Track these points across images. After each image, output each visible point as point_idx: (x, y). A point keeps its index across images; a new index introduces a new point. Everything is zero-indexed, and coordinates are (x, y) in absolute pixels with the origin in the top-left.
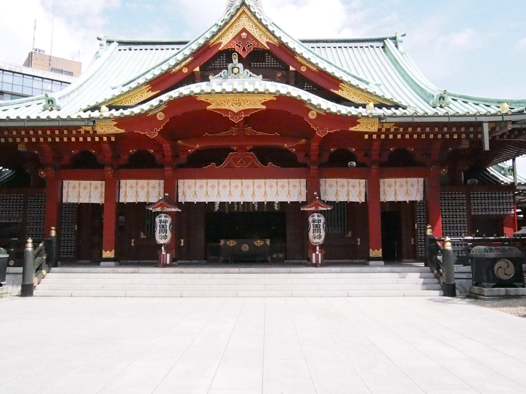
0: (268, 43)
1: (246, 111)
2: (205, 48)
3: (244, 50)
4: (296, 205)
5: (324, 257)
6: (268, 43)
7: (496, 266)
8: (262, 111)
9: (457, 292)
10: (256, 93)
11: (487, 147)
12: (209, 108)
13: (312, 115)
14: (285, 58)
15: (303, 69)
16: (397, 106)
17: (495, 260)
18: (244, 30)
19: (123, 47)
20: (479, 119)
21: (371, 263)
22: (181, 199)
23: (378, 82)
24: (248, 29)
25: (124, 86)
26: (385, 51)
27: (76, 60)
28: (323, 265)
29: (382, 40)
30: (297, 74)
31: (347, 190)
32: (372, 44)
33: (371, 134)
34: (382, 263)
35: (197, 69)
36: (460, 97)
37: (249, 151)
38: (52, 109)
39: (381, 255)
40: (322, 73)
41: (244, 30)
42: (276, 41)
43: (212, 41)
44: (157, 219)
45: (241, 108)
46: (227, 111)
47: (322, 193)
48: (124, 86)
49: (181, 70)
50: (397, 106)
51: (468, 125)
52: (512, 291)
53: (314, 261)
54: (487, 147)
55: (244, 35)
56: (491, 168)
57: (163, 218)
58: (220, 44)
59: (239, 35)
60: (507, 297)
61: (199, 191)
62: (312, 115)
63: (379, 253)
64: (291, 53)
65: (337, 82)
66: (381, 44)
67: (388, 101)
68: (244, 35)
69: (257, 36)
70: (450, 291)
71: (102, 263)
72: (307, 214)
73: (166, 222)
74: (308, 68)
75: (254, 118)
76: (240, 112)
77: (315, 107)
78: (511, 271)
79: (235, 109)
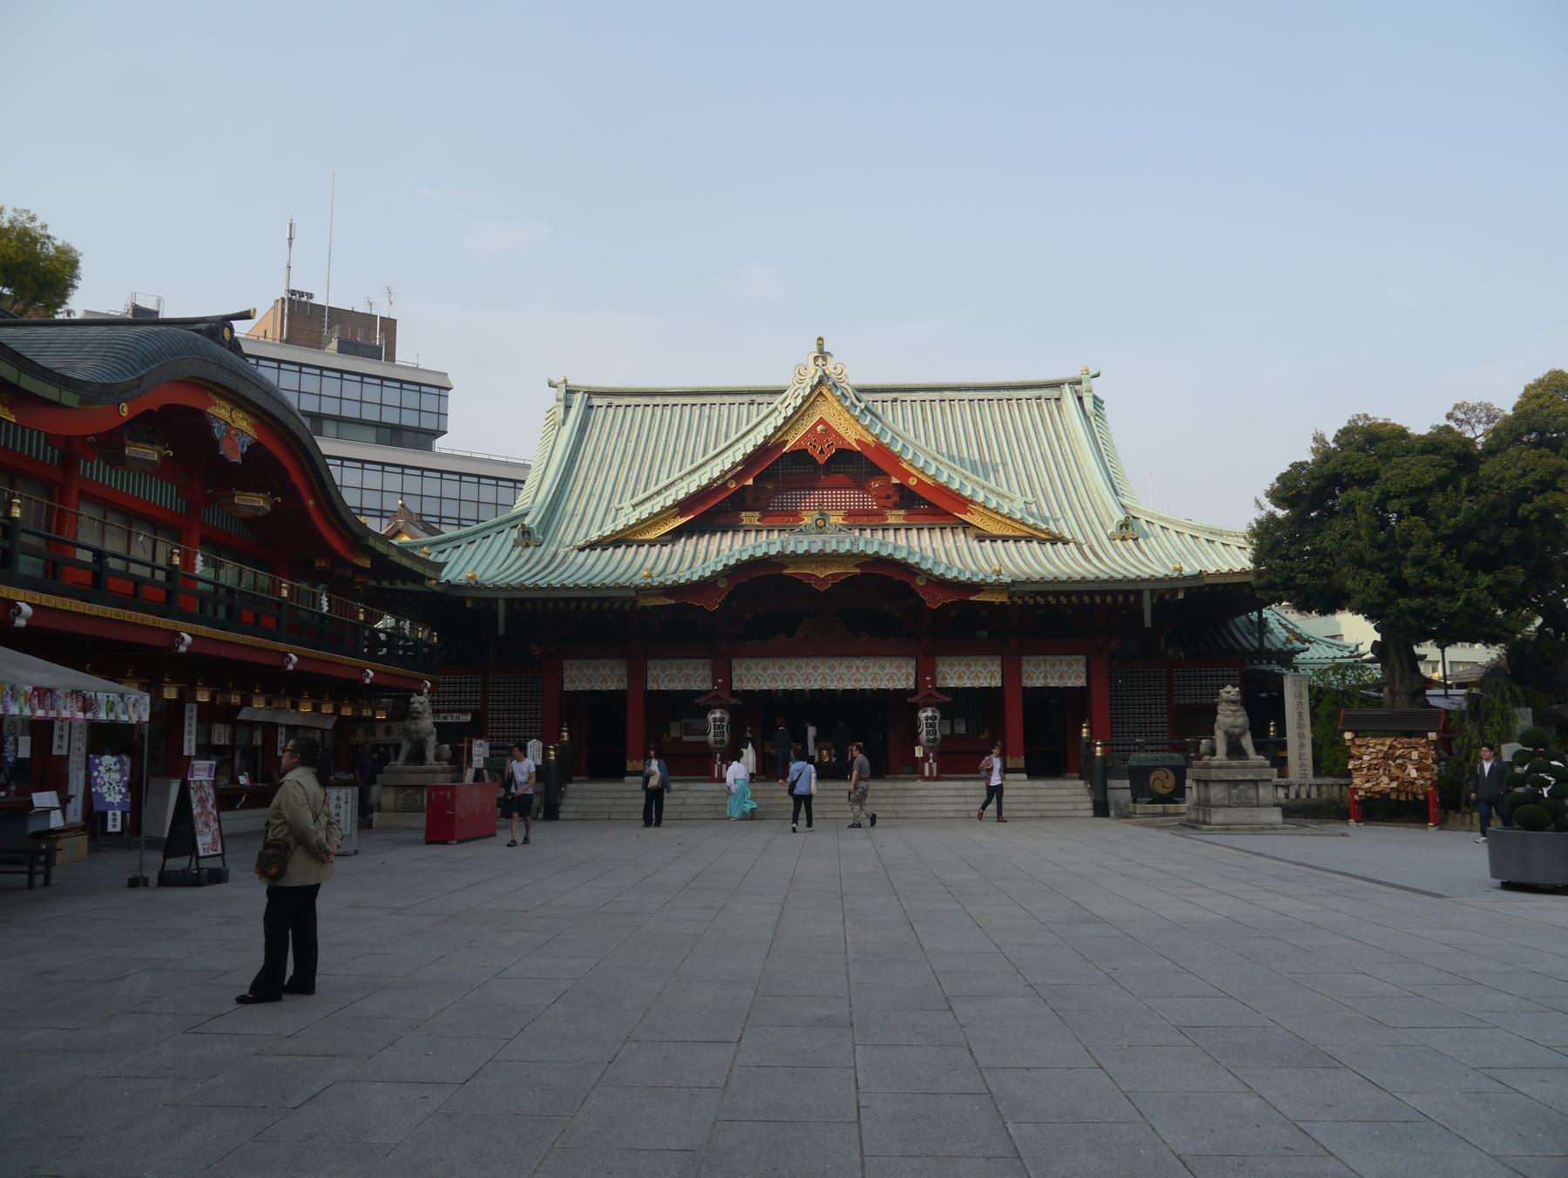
0: (858, 441)
2: (762, 451)
3: (822, 452)
5: (941, 770)
6: (858, 441)
7: (1152, 778)
8: (856, 575)
9: (1112, 813)
10: (849, 555)
11: (1148, 623)
13: (920, 582)
14: (884, 465)
15: (912, 482)
16: (1055, 540)
17: (1152, 769)
18: (821, 421)
19: (596, 401)
20: (1140, 587)
22: (736, 686)
23: (1030, 498)
24: (828, 419)
25: (634, 506)
26: (1059, 409)
27: (381, 311)
28: (938, 779)
29: (1057, 385)
30: (902, 488)
32: (1037, 393)
33: (1002, 603)
34: (1025, 776)
35: (750, 482)
36: (1160, 519)
38: (527, 546)
39: (1022, 765)
40: (943, 490)
41: (821, 421)
42: (870, 438)
44: (711, 717)
47: (939, 677)
48: (634, 506)
49: (725, 484)
50: (1055, 540)
51: (1126, 593)
52: (1171, 807)
53: (927, 773)
54: (1148, 623)
55: (820, 428)
56: (1237, 620)
57: (718, 715)
60: (1165, 814)
63: (1021, 762)
64: (895, 459)
65: (964, 503)
66: (1054, 393)
67: (1042, 531)
69: (841, 431)
70: (1101, 809)
71: (627, 779)
72: (916, 708)
73: (722, 720)
77: (924, 572)
78: (1171, 782)
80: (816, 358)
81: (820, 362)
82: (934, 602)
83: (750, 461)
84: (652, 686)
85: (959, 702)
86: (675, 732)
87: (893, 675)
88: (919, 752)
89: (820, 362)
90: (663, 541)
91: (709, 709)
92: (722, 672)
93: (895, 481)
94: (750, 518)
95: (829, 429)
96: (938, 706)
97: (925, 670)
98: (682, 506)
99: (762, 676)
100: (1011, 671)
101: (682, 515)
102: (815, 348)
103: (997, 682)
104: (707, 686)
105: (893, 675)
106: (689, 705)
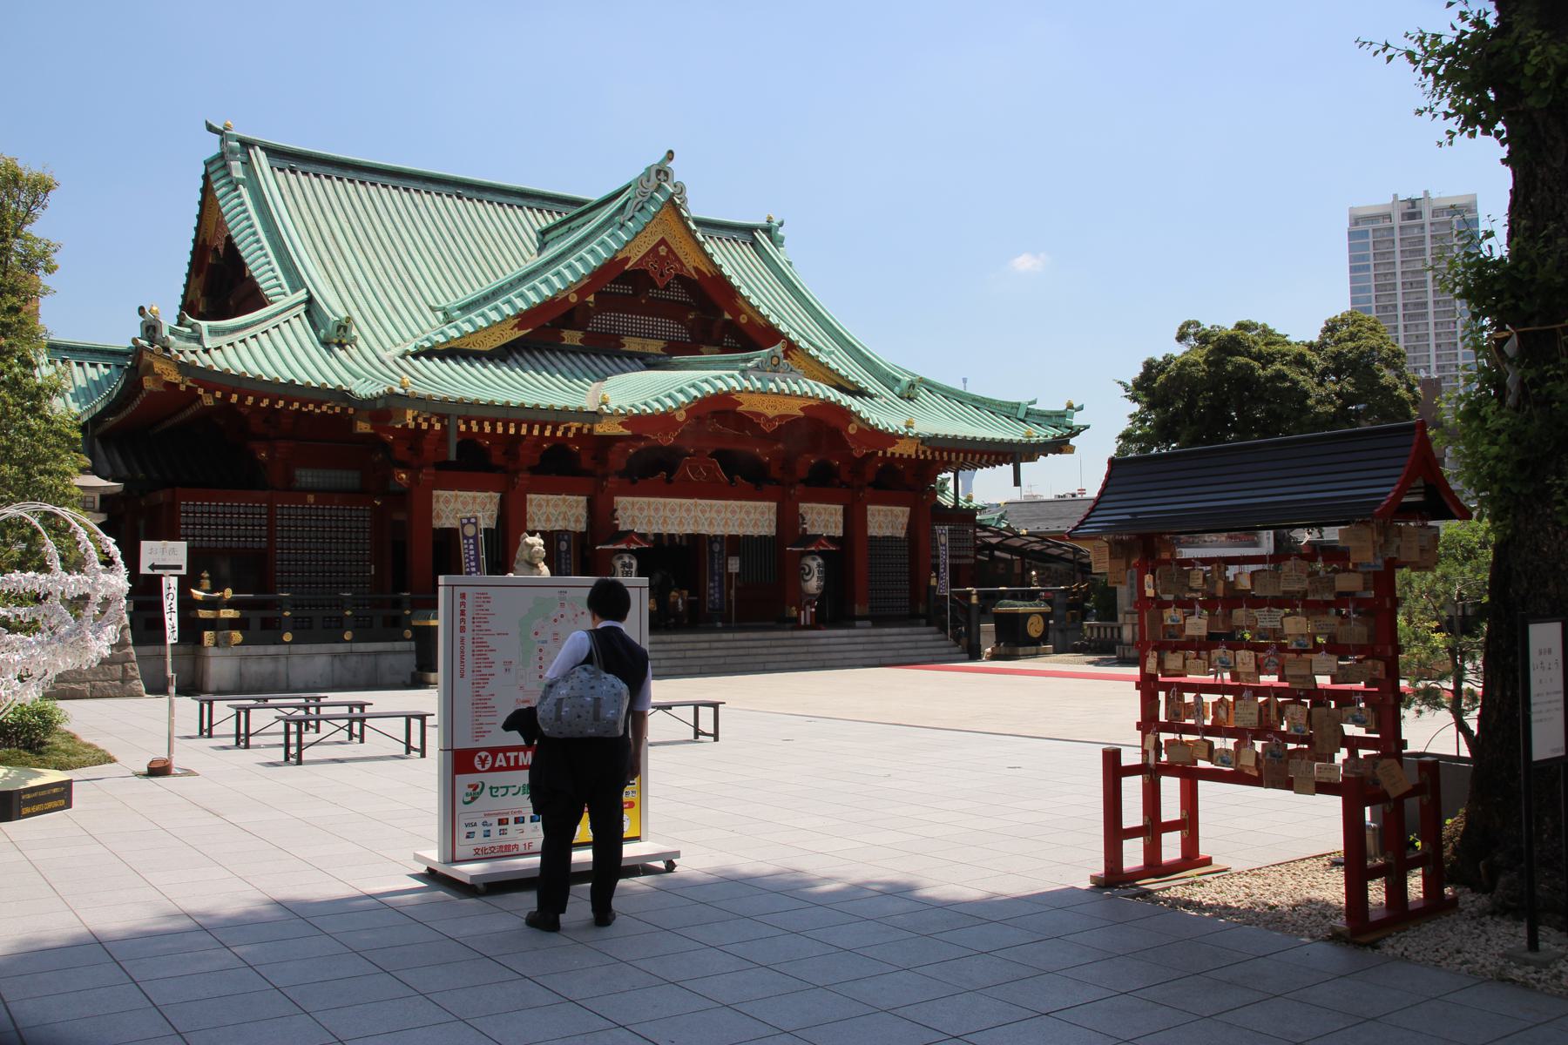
0: (696, 269)
1: (781, 417)
8: (799, 418)
12: (740, 408)
13: (852, 429)
15: (743, 319)
21: (858, 623)
24: (669, 241)
37: (711, 456)
41: (663, 242)
43: (620, 256)
45: (776, 413)
46: (759, 415)
58: (627, 259)
59: (654, 250)
62: (852, 429)
64: (731, 292)
67: (851, 383)
68: (663, 251)
74: (750, 319)
75: (789, 425)
76: (774, 419)
79: (771, 413)
80: (658, 172)
81: (662, 176)
83: (597, 275)
89: (662, 176)
90: (502, 355)
93: (727, 316)
94: (572, 337)
95: (670, 250)
98: (524, 318)
101: (520, 326)
102: (657, 157)
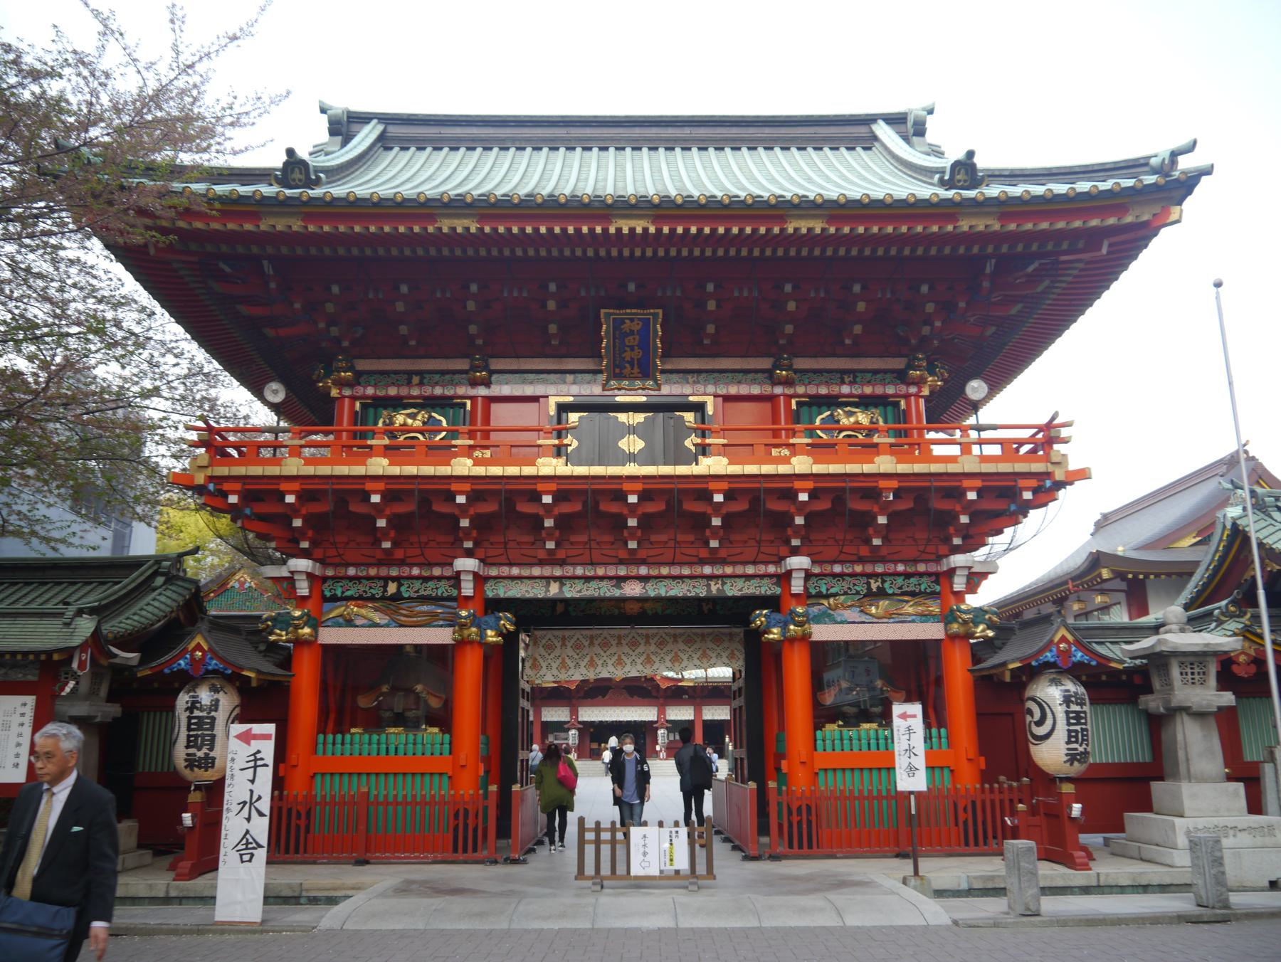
4: (652, 722)
22: (580, 719)
31: (682, 713)
61: (591, 714)
72: (657, 729)
82: (664, 686)
84: (544, 719)
85: (674, 726)
86: (551, 739)
87: (645, 714)
88: (658, 748)
91: (568, 730)
92: (574, 713)
96: (667, 728)
97: (661, 712)
99: (591, 714)
100: (698, 713)
103: (692, 718)
104: (568, 719)
105: (645, 714)
106: (560, 727)
